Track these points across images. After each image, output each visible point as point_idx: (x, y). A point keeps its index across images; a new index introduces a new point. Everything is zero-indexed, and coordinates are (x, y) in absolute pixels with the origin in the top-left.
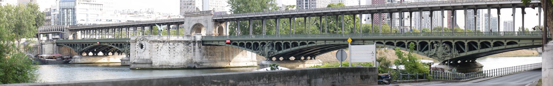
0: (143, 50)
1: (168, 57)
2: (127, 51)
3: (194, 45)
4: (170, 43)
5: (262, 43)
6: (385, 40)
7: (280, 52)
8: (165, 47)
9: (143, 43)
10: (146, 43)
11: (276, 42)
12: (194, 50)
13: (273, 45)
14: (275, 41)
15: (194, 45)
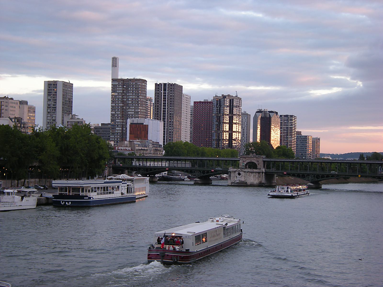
0: (240, 176)
1: (253, 180)
2: (198, 175)
3: (262, 174)
4: (254, 173)
5: (307, 175)
6: (377, 176)
7: (319, 180)
8: (252, 175)
9: (241, 173)
10: (243, 173)
11: (316, 175)
12: (262, 176)
13: (314, 176)
14: (316, 174)
15: (262, 174)
